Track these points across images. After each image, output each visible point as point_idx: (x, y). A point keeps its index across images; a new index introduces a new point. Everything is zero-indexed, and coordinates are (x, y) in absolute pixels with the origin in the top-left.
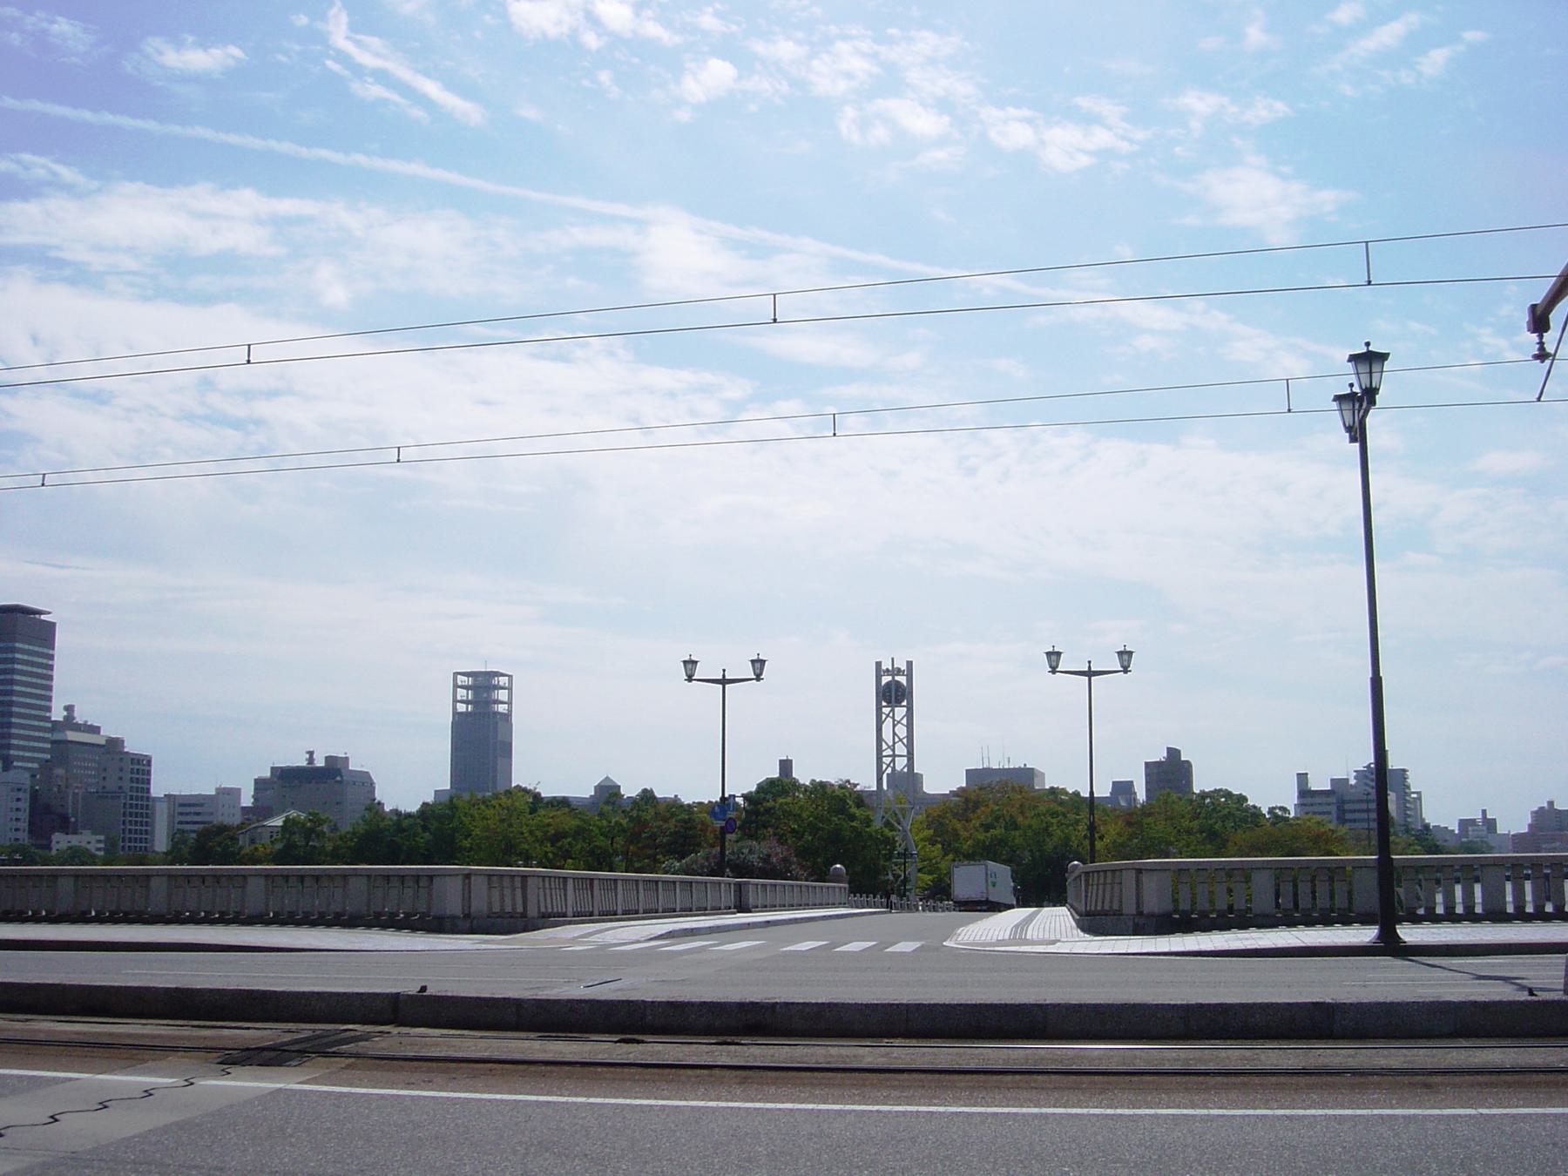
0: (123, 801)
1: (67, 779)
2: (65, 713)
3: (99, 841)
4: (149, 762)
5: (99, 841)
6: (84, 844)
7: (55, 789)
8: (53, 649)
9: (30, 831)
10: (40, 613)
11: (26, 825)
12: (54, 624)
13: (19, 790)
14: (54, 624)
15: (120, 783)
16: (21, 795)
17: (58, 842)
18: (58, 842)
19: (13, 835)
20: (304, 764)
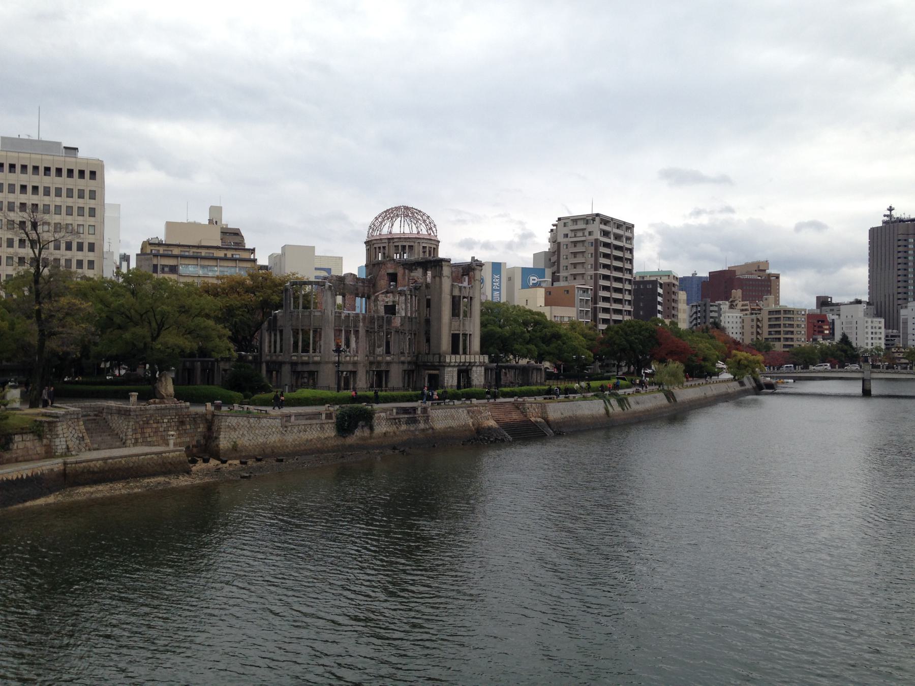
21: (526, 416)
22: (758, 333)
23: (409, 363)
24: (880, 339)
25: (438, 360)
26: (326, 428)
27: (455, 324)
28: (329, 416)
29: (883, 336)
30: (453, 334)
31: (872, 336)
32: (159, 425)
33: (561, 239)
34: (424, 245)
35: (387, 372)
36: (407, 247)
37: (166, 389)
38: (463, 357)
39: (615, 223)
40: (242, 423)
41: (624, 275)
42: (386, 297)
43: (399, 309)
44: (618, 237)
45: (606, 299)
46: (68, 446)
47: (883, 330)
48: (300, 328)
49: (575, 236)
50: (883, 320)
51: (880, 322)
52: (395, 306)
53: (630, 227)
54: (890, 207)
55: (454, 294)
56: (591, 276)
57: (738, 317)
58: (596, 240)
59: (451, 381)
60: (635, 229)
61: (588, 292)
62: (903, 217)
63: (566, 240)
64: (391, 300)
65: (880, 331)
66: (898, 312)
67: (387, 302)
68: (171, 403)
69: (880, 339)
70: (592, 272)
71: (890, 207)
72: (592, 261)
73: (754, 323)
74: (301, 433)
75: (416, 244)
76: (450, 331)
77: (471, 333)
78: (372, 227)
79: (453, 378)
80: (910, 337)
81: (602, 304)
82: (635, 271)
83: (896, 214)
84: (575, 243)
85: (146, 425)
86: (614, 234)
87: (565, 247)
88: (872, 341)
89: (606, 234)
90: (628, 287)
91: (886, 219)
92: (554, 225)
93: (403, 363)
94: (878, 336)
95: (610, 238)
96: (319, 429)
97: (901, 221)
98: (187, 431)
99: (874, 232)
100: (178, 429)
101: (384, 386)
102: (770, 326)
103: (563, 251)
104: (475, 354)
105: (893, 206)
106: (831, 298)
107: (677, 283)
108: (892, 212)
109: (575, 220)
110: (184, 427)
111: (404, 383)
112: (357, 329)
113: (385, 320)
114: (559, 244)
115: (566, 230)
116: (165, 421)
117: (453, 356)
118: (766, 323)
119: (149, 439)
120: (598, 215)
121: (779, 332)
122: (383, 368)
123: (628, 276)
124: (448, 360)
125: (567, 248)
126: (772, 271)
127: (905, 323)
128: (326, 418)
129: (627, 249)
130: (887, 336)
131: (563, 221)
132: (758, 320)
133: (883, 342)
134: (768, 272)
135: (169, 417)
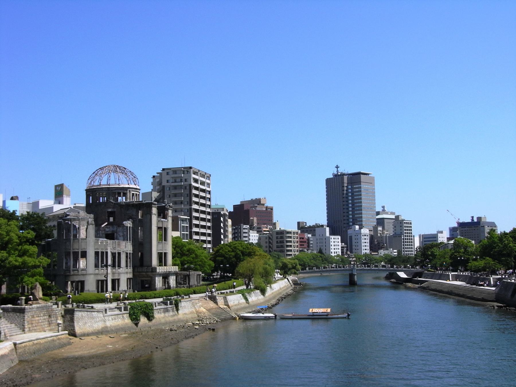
0: (403, 238)
1: (383, 231)
2: (382, 209)
3: (395, 252)
4: (411, 223)
5: (395, 252)
6: (390, 253)
7: (379, 235)
8: (374, 186)
9: (371, 250)
10: (369, 174)
11: (369, 248)
12: (374, 177)
13: (365, 235)
14: (374, 177)
15: (401, 231)
16: (366, 237)
17: (381, 253)
18: (381, 253)
19: (364, 252)
20: (470, 221)
21: (217, 304)
22: (270, 247)
23: (130, 273)
24: (338, 249)
25: (150, 270)
26: (125, 317)
27: (160, 246)
28: (126, 309)
29: (340, 247)
30: (158, 253)
31: (334, 247)
32: (39, 318)
33: (164, 183)
34: (133, 192)
35: (119, 280)
36: (122, 194)
37: (39, 294)
38: (165, 267)
39: (200, 173)
40: (84, 315)
41: (199, 208)
42: (107, 228)
43: (117, 237)
44: (203, 183)
45: (197, 226)
46: (5, 333)
47: (340, 244)
48: (72, 251)
49: (175, 182)
50: (340, 237)
51: (338, 238)
52: (114, 234)
53: (209, 178)
54: (337, 166)
55: (158, 226)
56: (188, 210)
57: (256, 236)
58: (191, 185)
59: (159, 284)
60: (211, 178)
61: (186, 221)
62: (344, 172)
63: (168, 184)
64: (111, 230)
65: (338, 244)
66: (347, 231)
67: (107, 231)
68: (42, 303)
69: (338, 249)
70: (188, 207)
71: (337, 166)
72: (188, 199)
73: (267, 240)
74: (114, 321)
75: (128, 191)
76: (157, 250)
77: (168, 252)
78: (92, 178)
79: (160, 282)
80: (354, 247)
81: (195, 229)
82: (212, 207)
83: (341, 170)
84: (175, 188)
85: (33, 319)
86: (201, 180)
87: (168, 189)
88: (334, 251)
89: (196, 181)
90: (209, 217)
91: (336, 173)
92: (158, 173)
93: (127, 273)
94: (337, 247)
95: (198, 184)
96: (122, 317)
97: (343, 175)
98: (53, 322)
99: (328, 181)
100: (48, 321)
101: (117, 290)
102: (277, 242)
103: (167, 193)
104: (170, 266)
105: (338, 165)
106: (306, 223)
107: (227, 214)
108: (338, 169)
109: (175, 171)
110: (51, 319)
111: (127, 286)
112: (107, 251)
113: (117, 243)
114: (164, 187)
115: (168, 177)
116: (42, 315)
117: (161, 267)
118: (275, 240)
119: (35, 328)
120: (191, 168)
121: (282, 246)
122: (116, 278)
123: (208, 210)
124: (158, 271)
125: (169, 190)
126: (268, 204)
127: (351, 237)
128: (124, 310)
129: (207, 191)
130: (342, 247)
131: (166, 171)
132: (270, 238)
133: (340, 251)
134: (266, 205)
135: (43, 313)
